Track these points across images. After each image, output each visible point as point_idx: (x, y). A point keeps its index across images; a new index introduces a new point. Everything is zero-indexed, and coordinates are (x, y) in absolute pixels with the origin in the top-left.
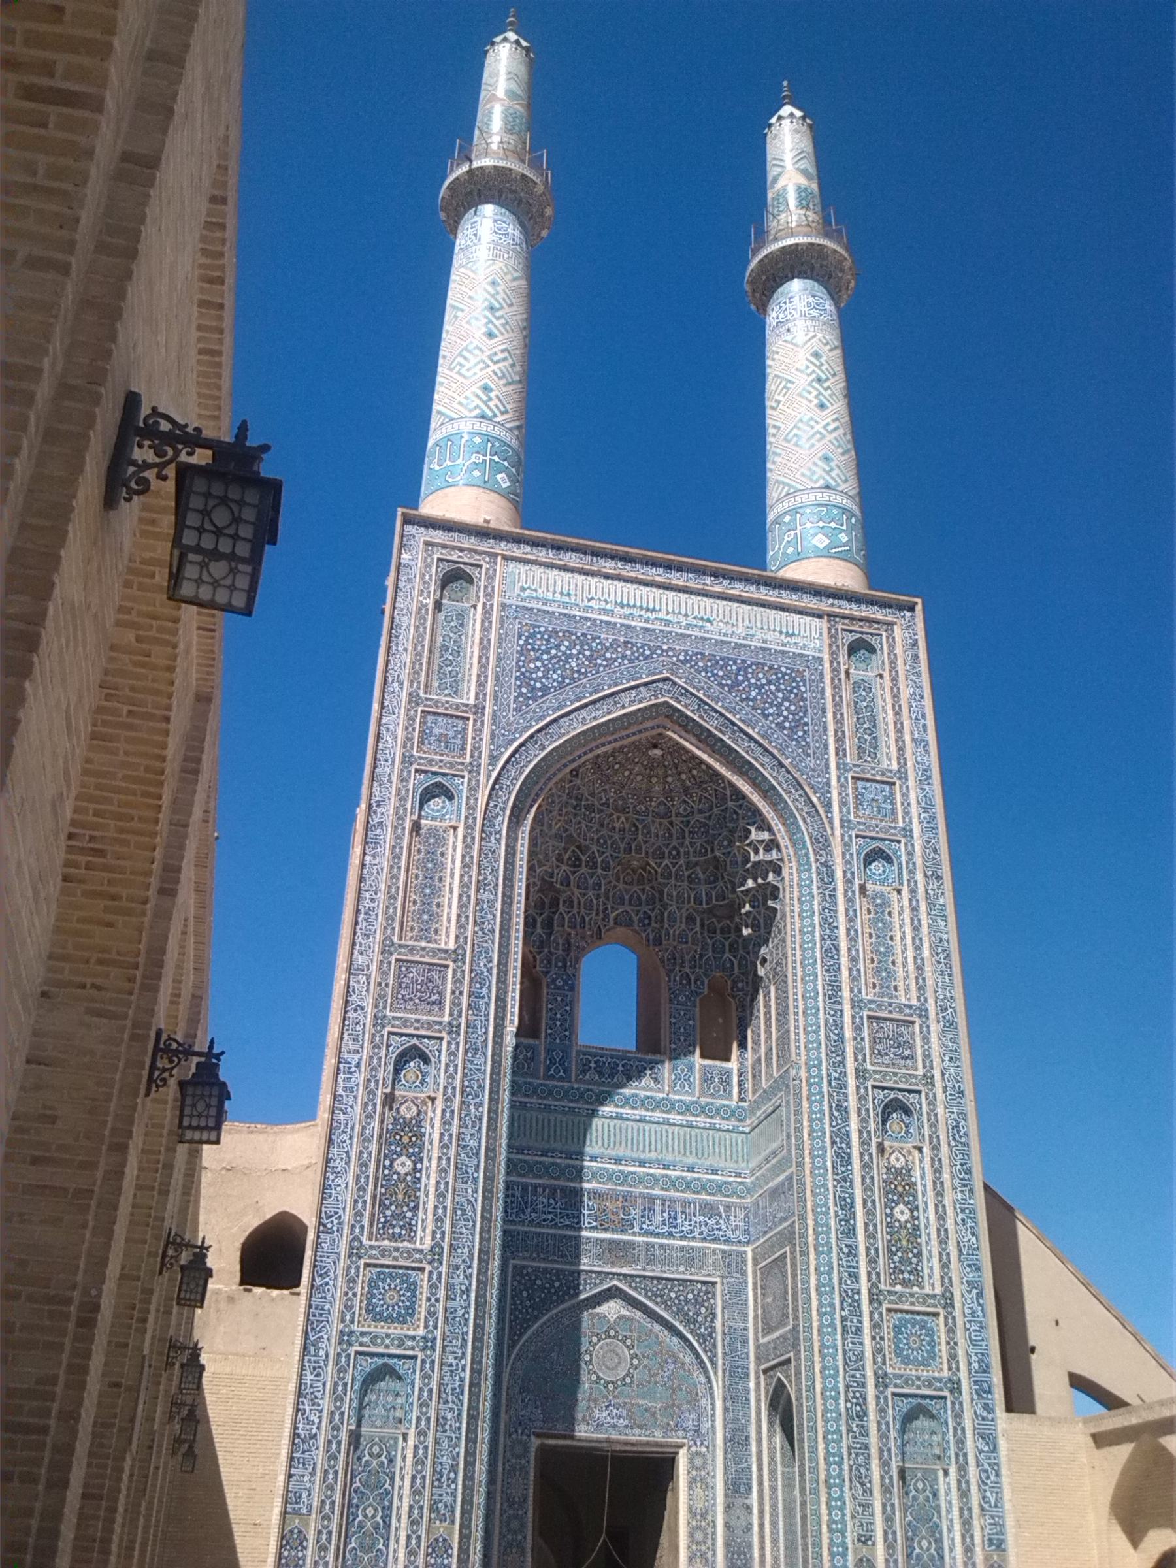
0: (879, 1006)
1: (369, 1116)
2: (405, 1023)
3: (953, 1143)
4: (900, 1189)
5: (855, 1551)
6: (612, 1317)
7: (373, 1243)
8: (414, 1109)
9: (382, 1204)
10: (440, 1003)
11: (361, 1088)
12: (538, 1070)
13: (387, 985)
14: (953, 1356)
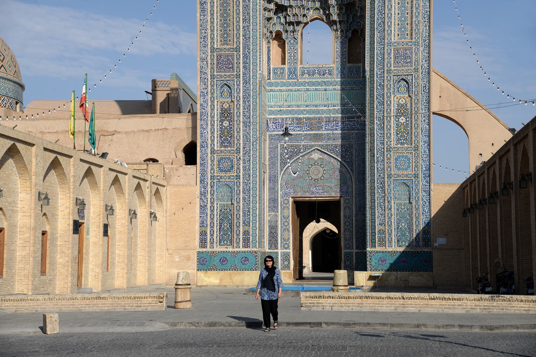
0: (399, 44)
1: (212, 110)
2: (221, 76)
3: (423, 93)
4: (402, 111)
5: (378, 227)
6: (316, 158)
7: (219, 149)
8: (228, 105)
9: (220, 137)
10: (233, 67)
11: (209, 101)
12: (285, 76)
13: (214, 64)
14: (416, 166)
